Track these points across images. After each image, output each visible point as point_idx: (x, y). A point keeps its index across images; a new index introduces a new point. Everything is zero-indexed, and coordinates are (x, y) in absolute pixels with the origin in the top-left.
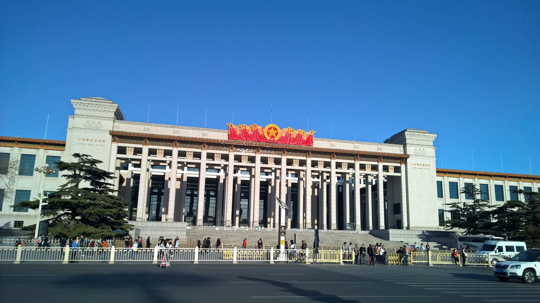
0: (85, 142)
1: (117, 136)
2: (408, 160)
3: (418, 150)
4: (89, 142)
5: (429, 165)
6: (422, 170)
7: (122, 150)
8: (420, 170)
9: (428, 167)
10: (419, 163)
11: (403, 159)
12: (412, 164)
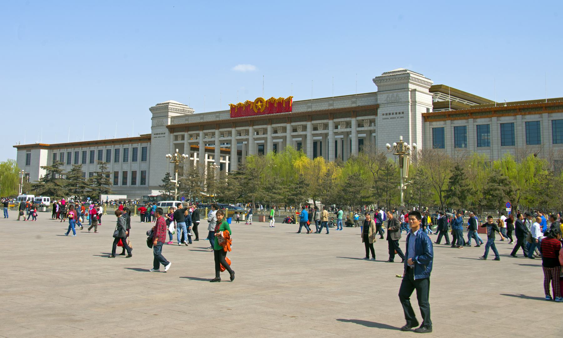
0: (157, 136)
1: (172, 129)
2: (379, 111)
3: (390, 96)
4: (159, 136)
5: (403, 113)
6: (394, 120)
7: (176, 138)
8: (392, 120)
9: (401, 115)
10: (391, 112)
11: (373, 110)
12: (383, 115)
